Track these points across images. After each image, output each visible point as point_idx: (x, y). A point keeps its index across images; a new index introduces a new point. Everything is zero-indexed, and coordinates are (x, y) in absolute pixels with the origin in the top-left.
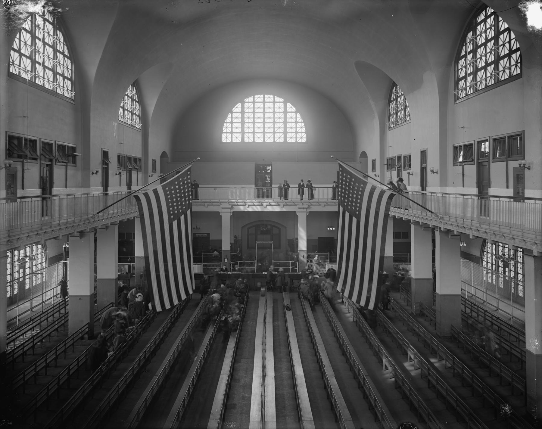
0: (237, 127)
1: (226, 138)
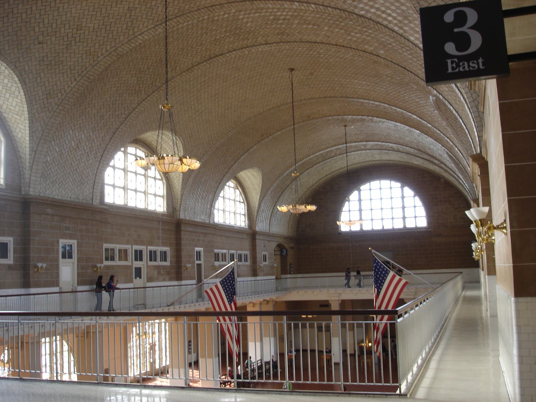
0: (355, 216)
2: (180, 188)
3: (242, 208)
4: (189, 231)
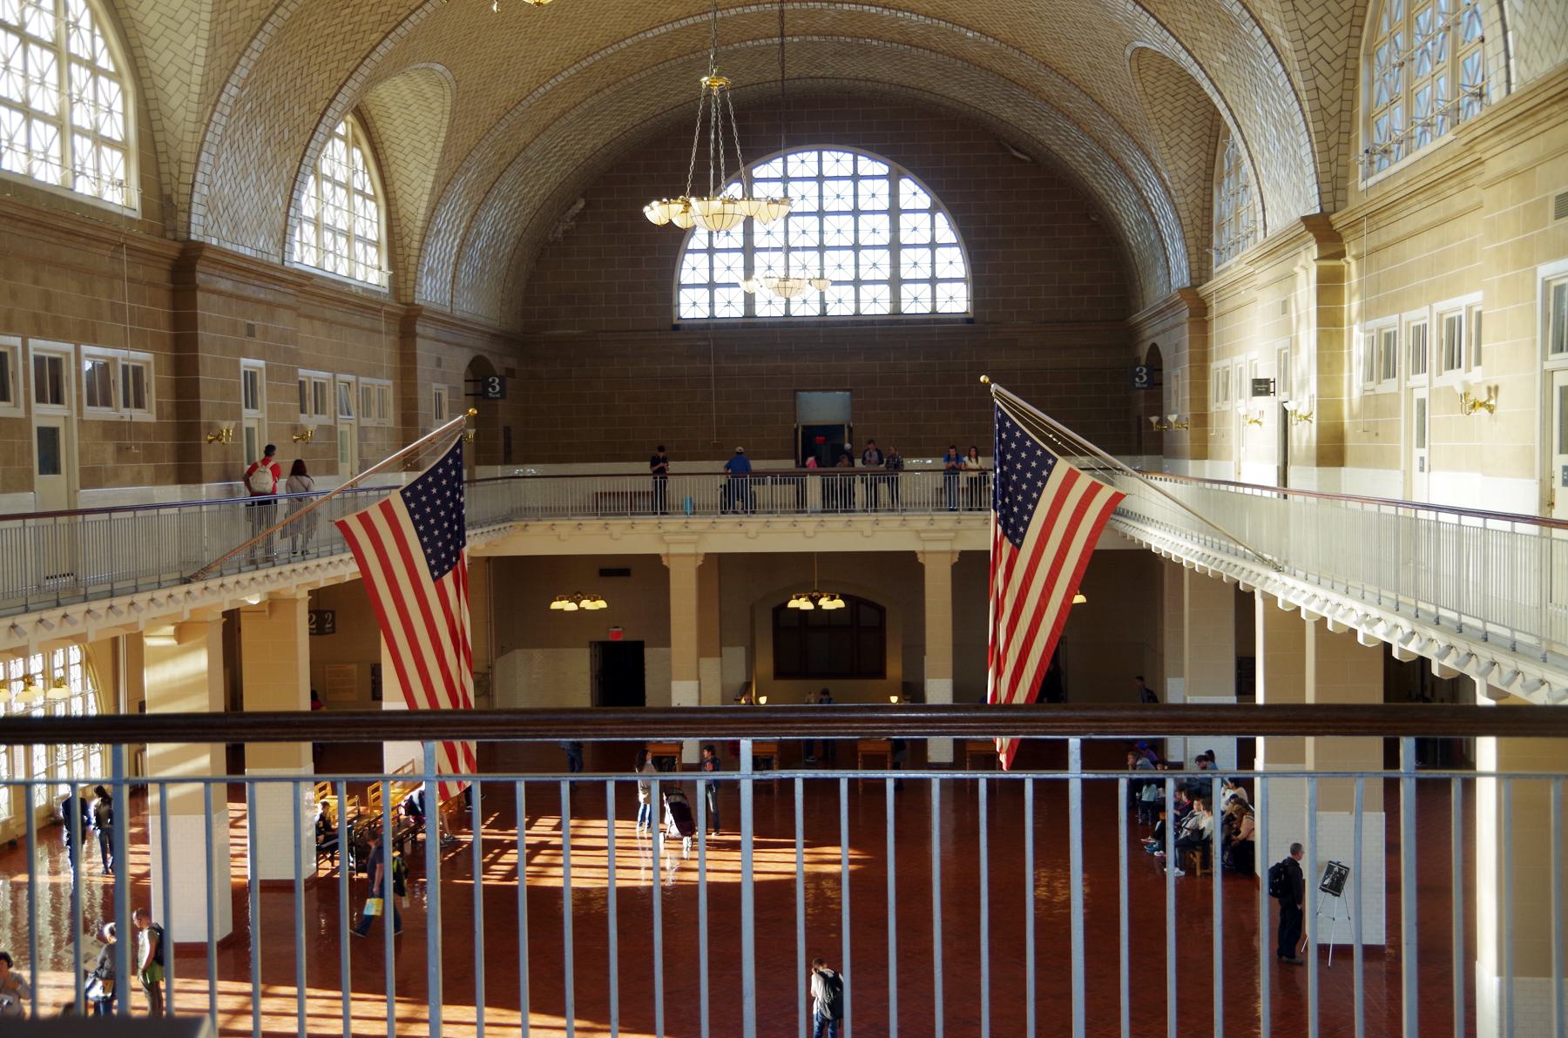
1: (692, 305)
2: (192, 117)
3: (370, 220)
4: (220, 293)
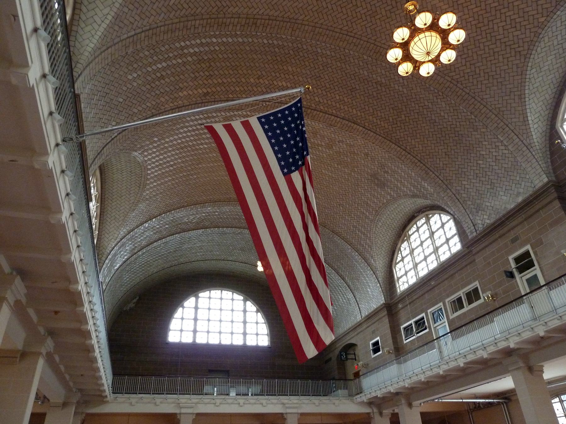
0: (189, 325)
1: (173, 337)
